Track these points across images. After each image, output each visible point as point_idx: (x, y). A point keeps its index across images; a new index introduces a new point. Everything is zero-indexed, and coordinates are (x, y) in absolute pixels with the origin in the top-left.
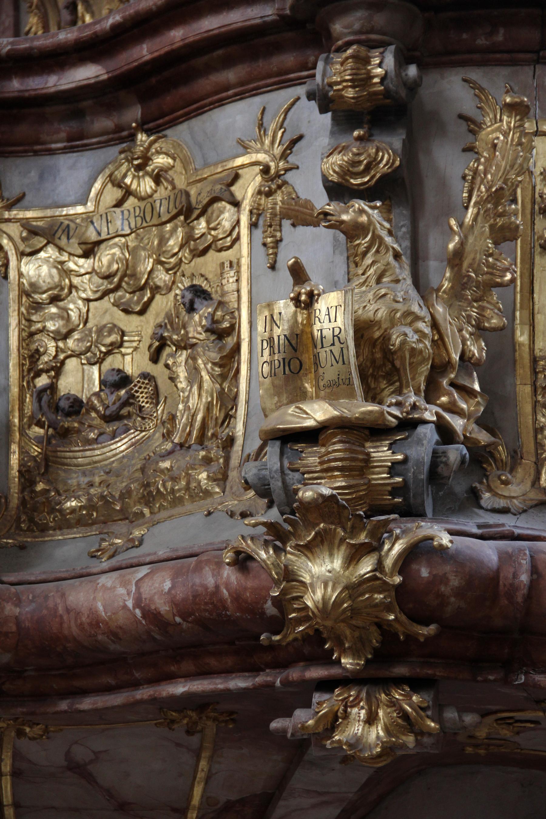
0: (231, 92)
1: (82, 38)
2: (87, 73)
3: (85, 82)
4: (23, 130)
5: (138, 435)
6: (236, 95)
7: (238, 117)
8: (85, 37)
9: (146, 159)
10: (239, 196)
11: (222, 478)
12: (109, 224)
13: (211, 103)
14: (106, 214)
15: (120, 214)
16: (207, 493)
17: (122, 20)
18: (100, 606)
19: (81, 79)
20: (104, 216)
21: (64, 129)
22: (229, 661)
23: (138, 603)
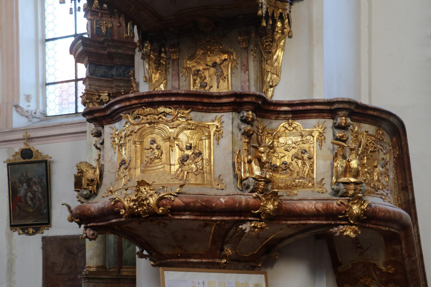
4: (268, 115)
9: (292, 124)
10: (314, 135)
11: (313, 185)
16: (311, 187)
18: (306, 207)
21: (275, 116)
22: (324, 218)
23: (315, 208)
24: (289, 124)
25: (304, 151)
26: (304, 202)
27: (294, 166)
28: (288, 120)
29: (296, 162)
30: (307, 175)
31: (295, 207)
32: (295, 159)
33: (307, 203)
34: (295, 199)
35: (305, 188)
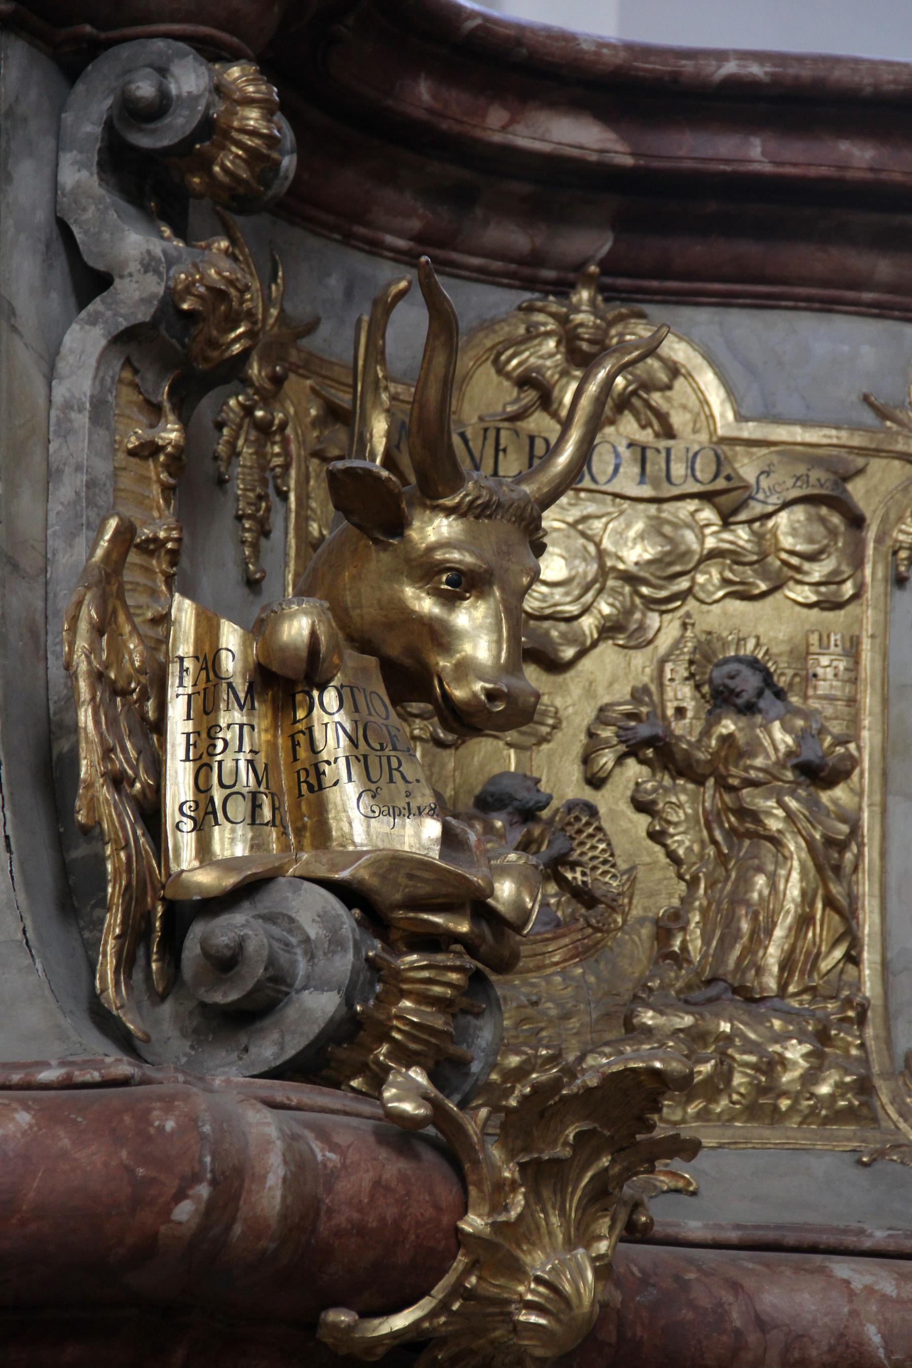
0: (867, 296)
1: (637, 69)
2: (576, 135)
3: (576, 152)
5: (588, 937)
6: (870, 305)
7: (865, 349)
8: (645, 70)
12: (501, 454)
13: (809, 299)
14: (498, 430)
15: (526, 442)
17: (766, 79)
19: (564, 141)
20: (492, 434)
24: (569, 338)
25: (750, 682)
26: (842, 1268)
27: (621, 844)
28: (563, 289)
29: (642, 806)
30: (787, 964)
31: (736, 1318)
32: (633, 769)
33: (888, 1287)
34: (694, 1228)
35: (776, 1116)
